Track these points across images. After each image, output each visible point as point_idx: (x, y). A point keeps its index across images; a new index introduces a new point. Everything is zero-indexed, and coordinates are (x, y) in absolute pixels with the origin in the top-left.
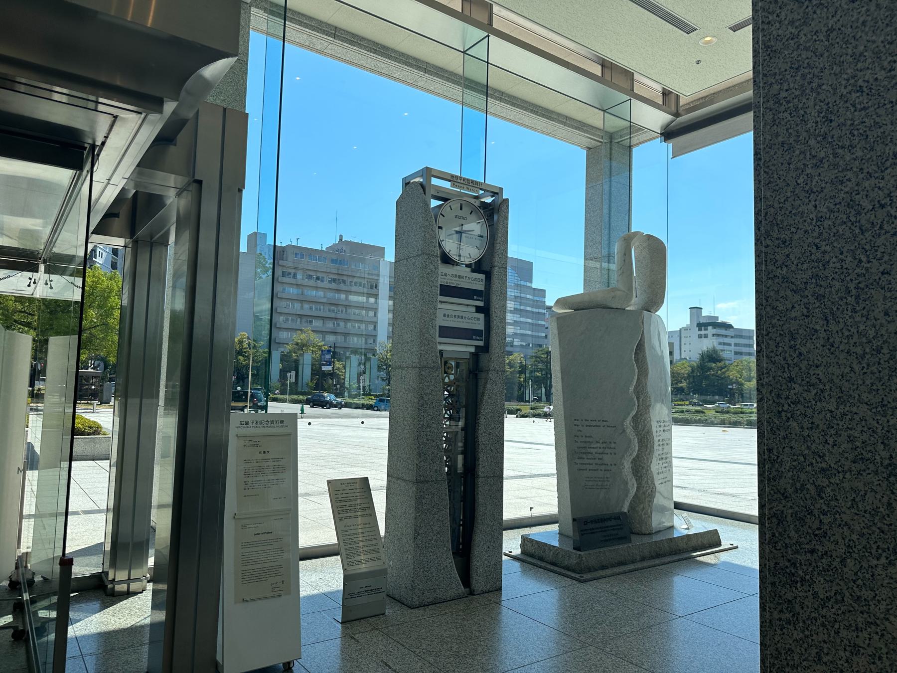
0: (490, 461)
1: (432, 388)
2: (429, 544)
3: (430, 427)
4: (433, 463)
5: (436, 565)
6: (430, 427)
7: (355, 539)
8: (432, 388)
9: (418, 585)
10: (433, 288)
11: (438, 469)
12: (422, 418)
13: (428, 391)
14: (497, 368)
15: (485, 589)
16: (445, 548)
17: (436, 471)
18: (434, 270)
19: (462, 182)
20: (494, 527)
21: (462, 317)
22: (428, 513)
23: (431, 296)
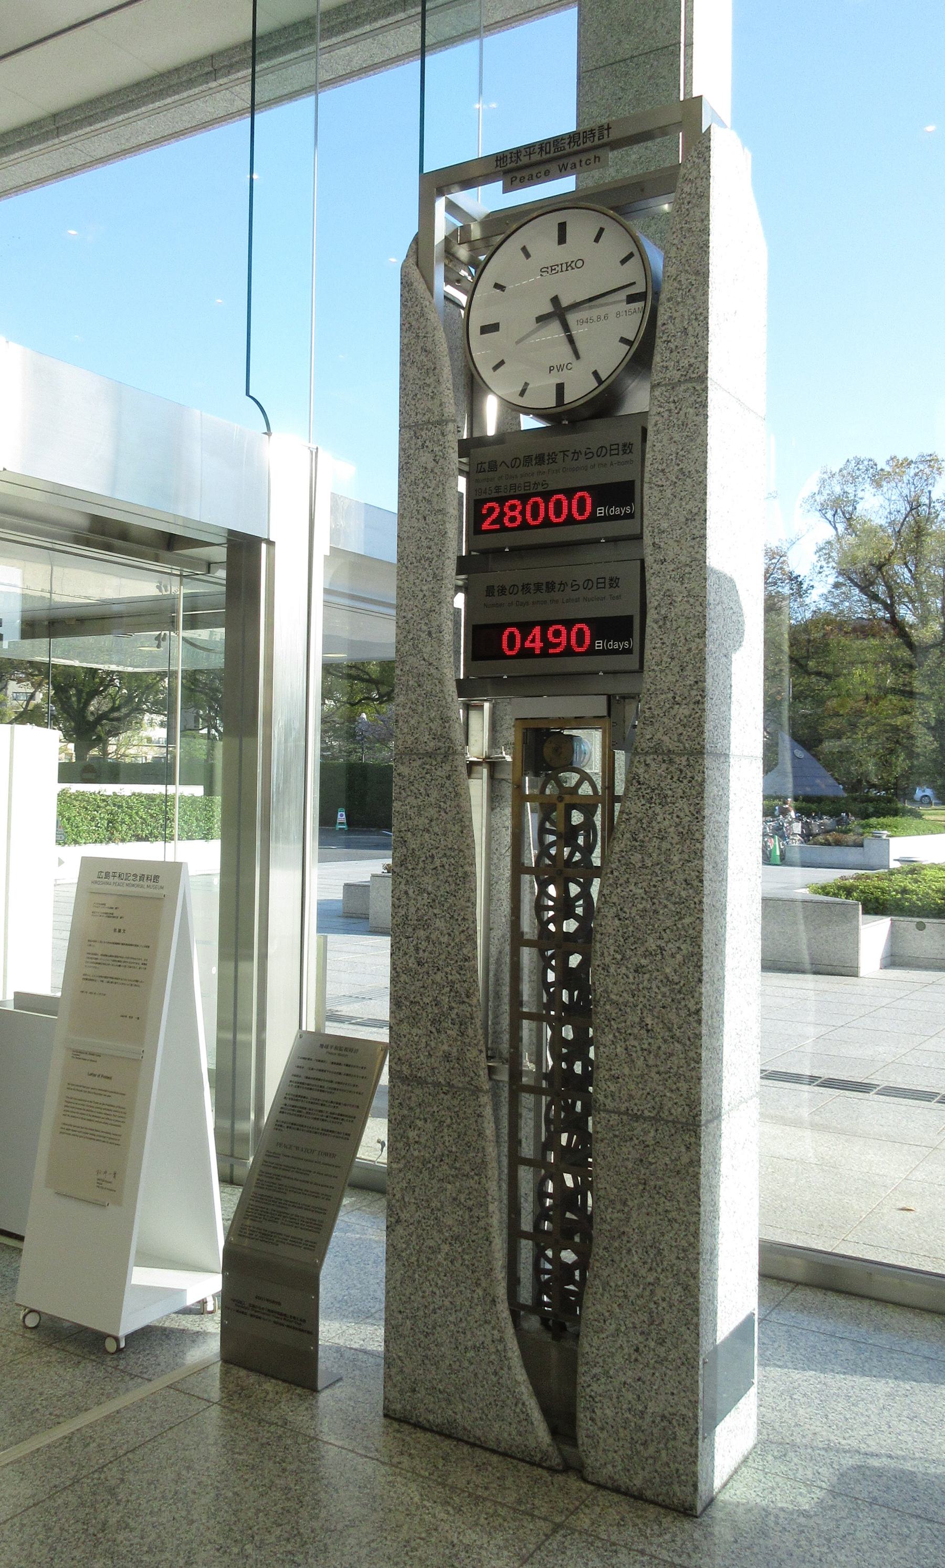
0: (640, 1063)
1: (432, 812)
2: (429, 1259)
3: (426, 926)
4: (439, 1031)
5: (452, 1327)
6: (426, 926)
7: (285, 1182)
8: (432, 812)
9: (399, 1357)
10: (430, 519)
11: (454, 1052)
12: (404, 898)
13: (422, 822)
14: (668, 743)
15: (623, 1480)
16: (480, 1292)
17: (447, 1057)
18: (431, 465)
19: (536, 157)
20: (659, 1293)
21: (550, 586)
22: (426, 1173)
23: (425, 543)
